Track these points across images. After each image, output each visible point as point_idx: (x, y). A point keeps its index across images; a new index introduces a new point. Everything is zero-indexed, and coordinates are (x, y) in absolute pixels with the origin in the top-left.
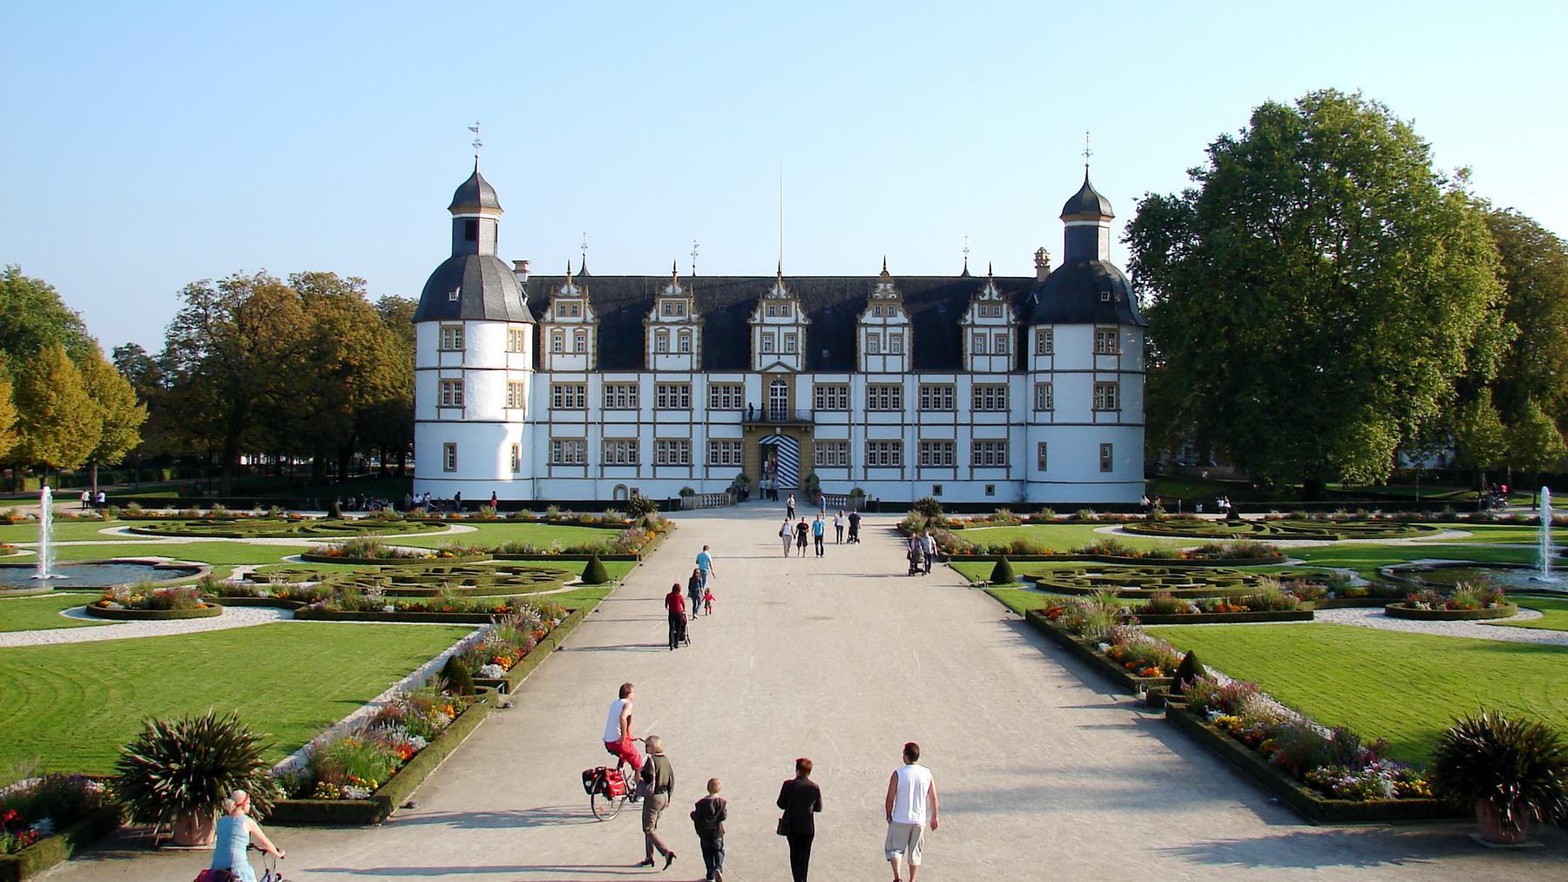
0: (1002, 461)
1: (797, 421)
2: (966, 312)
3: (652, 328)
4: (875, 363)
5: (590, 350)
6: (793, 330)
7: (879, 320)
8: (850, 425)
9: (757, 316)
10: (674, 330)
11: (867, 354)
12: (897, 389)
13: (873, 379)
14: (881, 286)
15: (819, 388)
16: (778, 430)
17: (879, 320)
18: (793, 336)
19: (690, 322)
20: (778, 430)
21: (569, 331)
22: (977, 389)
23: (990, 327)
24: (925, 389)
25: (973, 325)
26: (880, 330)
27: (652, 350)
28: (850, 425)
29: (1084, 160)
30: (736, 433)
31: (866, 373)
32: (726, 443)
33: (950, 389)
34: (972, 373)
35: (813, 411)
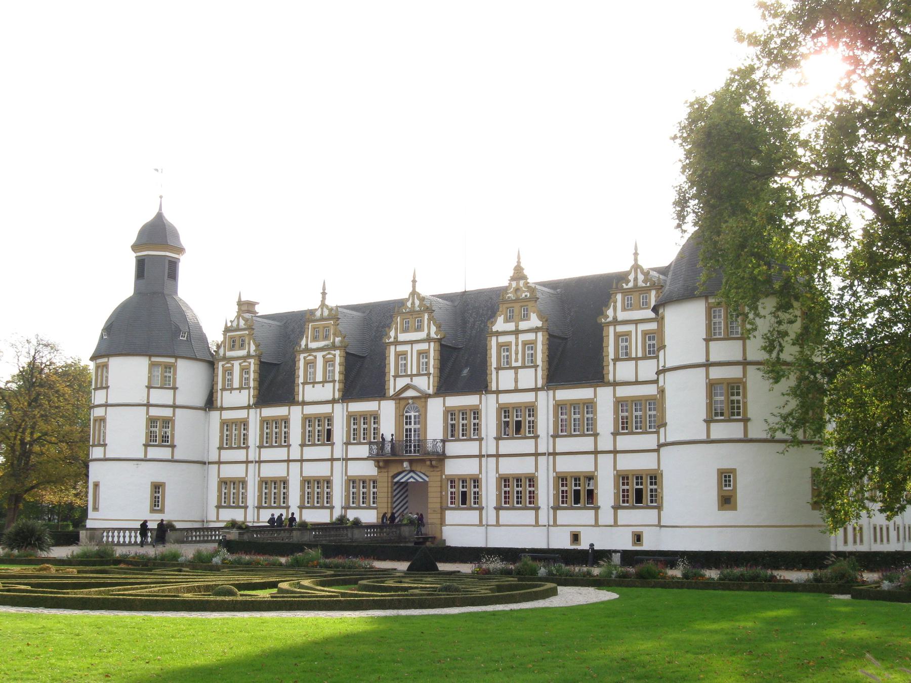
0: (656, 501)
1: (428, 453)
2: (608, 307)
3: (302, 356)
4: (505, 380)
5: (252, 384)
6: (424, 346)
7: (511, 326)
9: (392, 334)
10: (320, 355)
11: (498, 369)
12: (531, 409)
13: (505, 399)
14: (514, 284)
15: (450, 413)
16: (406, 464)
17: (511, 326)
18: (423, 354)
19: (334, 347)
20: (406, 464)
21: (236, 364)
22: (620, 403)
23: (636, 322)
24: (560, 407)
25: (615, 322)
26: (511, 338)
27: (301, 380)
28: (480, 456)
30: (368, 469)
31: (498, 392)
32: (364, 481)
33: (590, 405)
34: (615, 384)
35: (444, 441)
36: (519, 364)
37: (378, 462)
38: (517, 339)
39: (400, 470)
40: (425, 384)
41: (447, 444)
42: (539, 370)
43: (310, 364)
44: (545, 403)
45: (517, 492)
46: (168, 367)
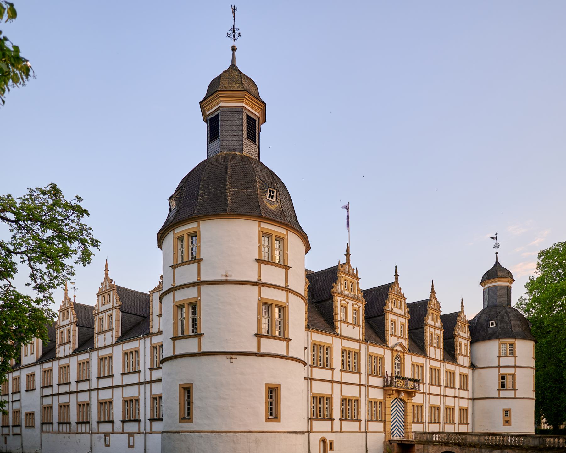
3: (339, 298)
26: (432, 330)
29: (495, 250)
34: (460, 366)
36: (435, 345)
37: (384, 390)
40: (406, 343)
43: (345, 308)
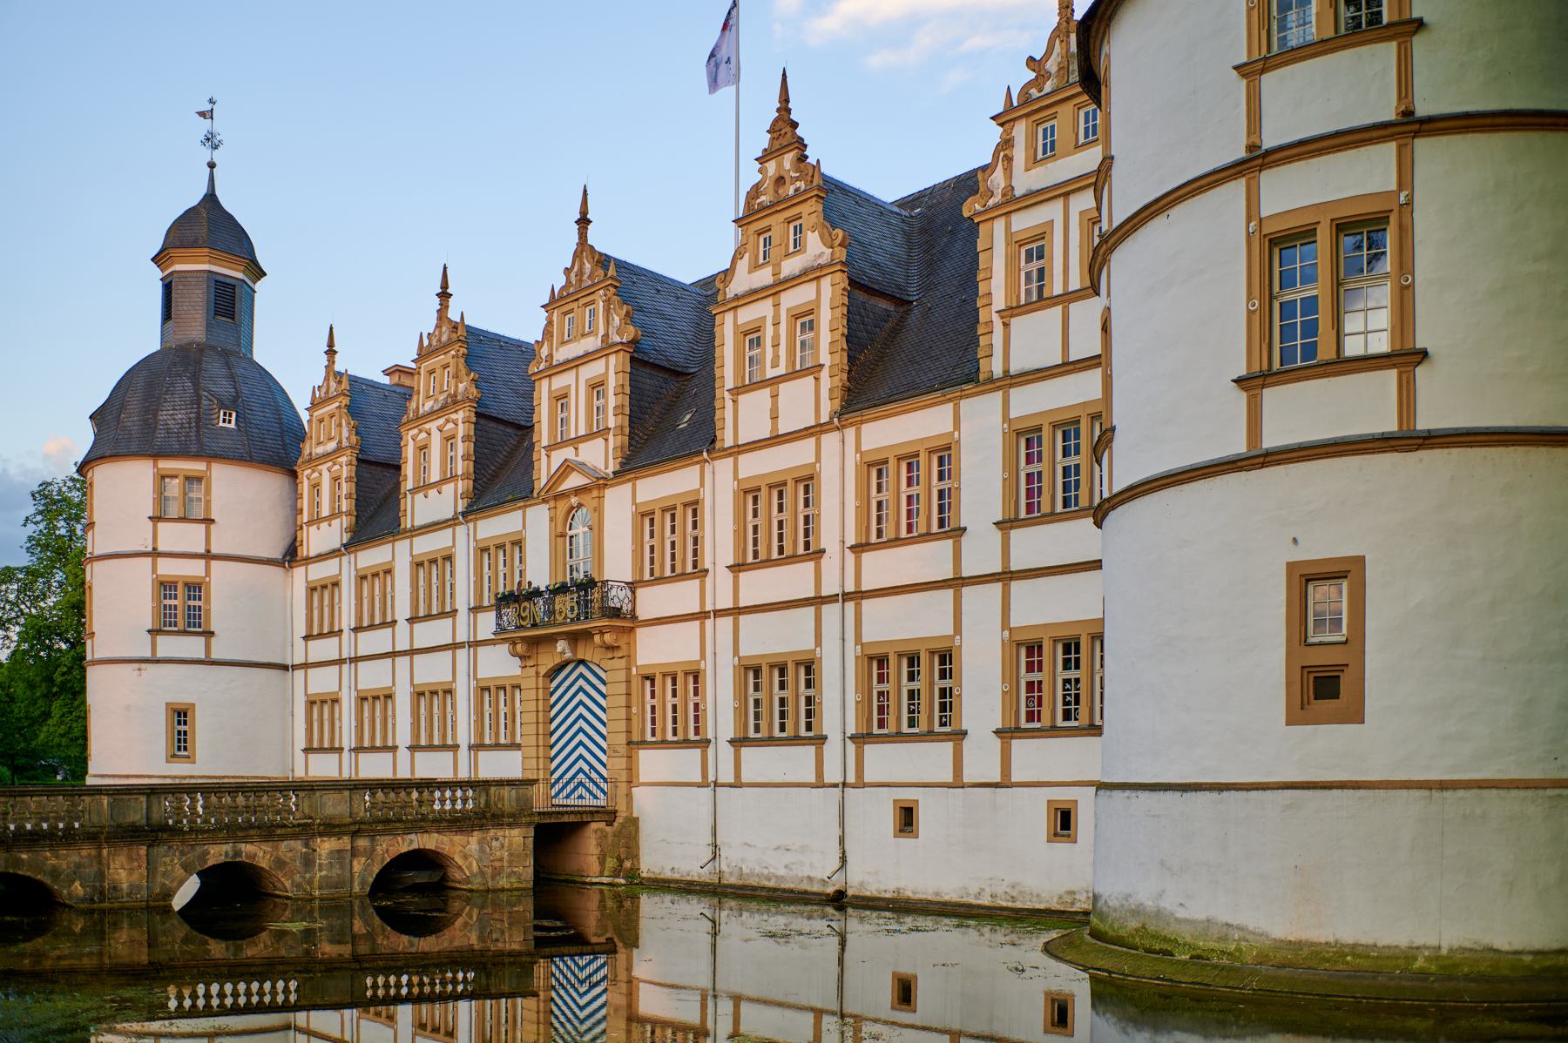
7: (765, 277)
8: (702, 616)
20: (561, 645)
35: (632, 586)
38: (776, 305)
39: (558, 660)
41: (639, 592)
42: (825, 375)
44: (836, 462)
45: (780, 699)
46: (191, 479)
